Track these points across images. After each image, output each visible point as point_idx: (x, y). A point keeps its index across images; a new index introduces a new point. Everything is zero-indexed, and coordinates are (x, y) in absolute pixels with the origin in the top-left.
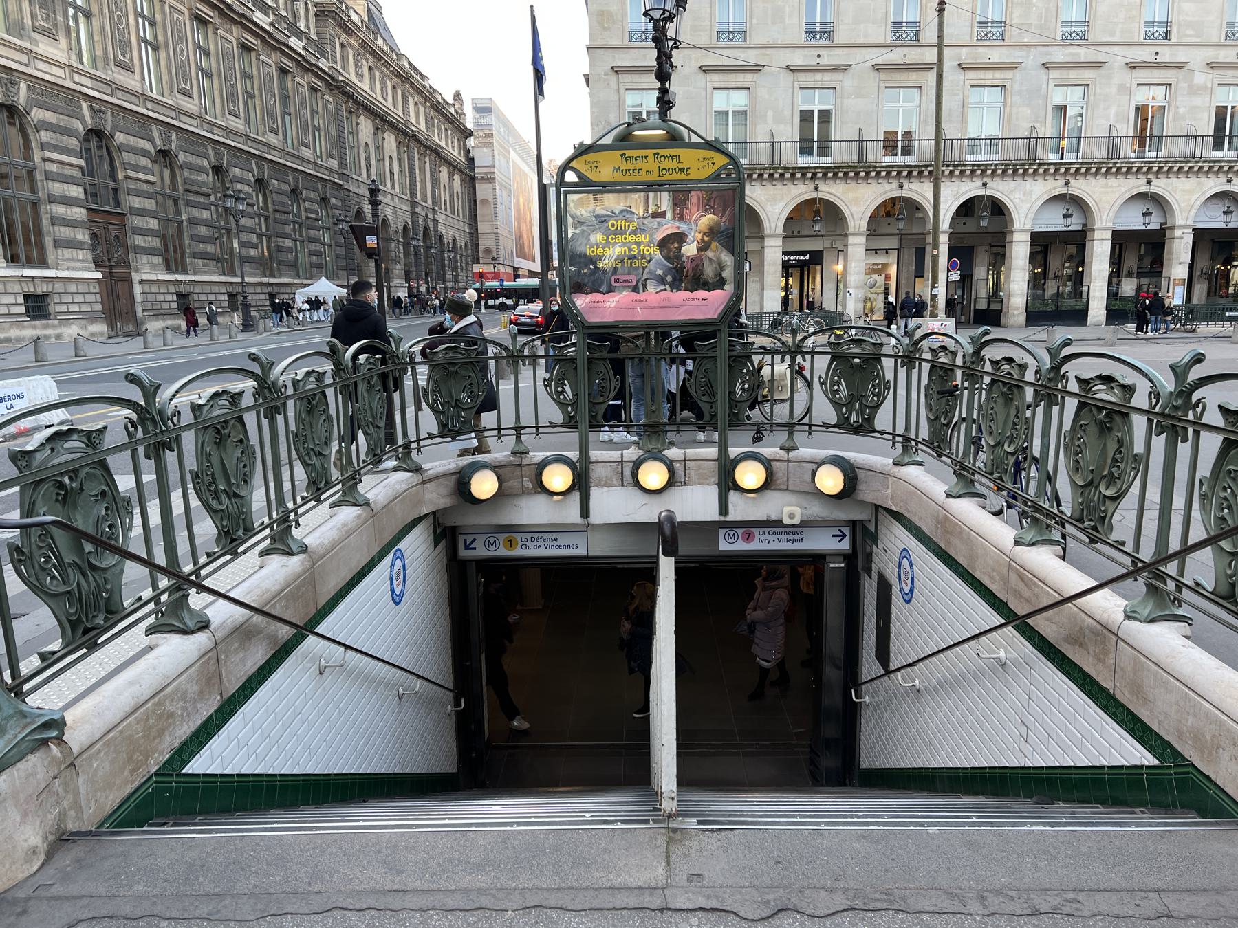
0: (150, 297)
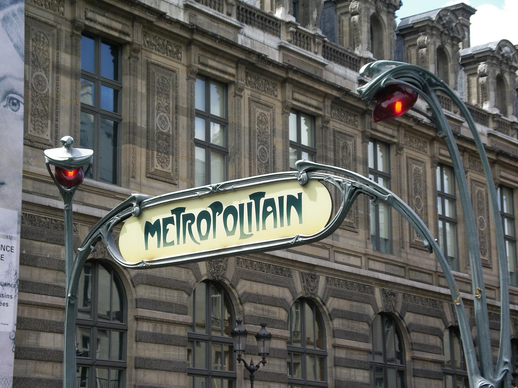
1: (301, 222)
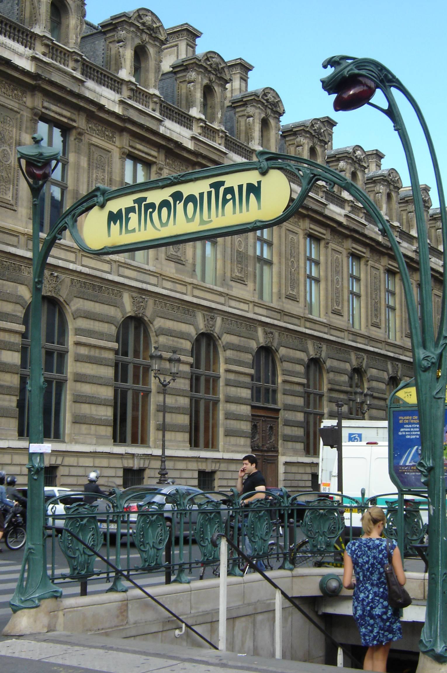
0: (290, 476)
1: (259, 208)
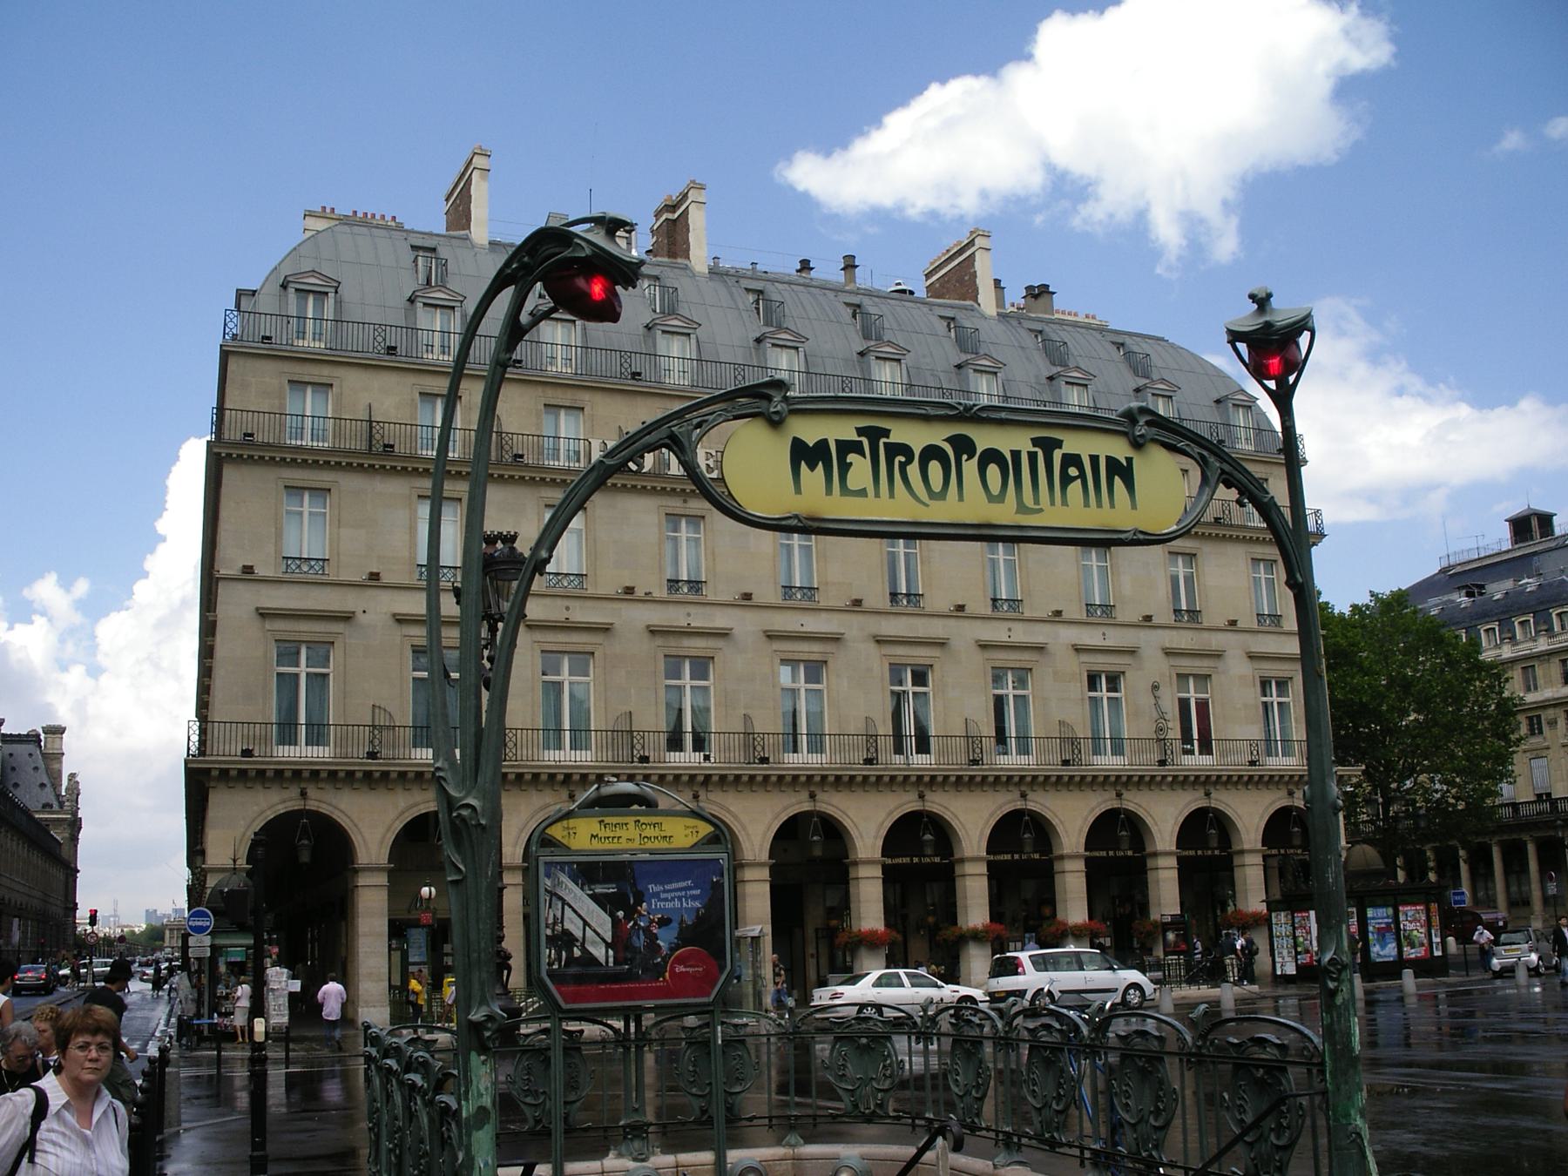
1: (1134, 506)
